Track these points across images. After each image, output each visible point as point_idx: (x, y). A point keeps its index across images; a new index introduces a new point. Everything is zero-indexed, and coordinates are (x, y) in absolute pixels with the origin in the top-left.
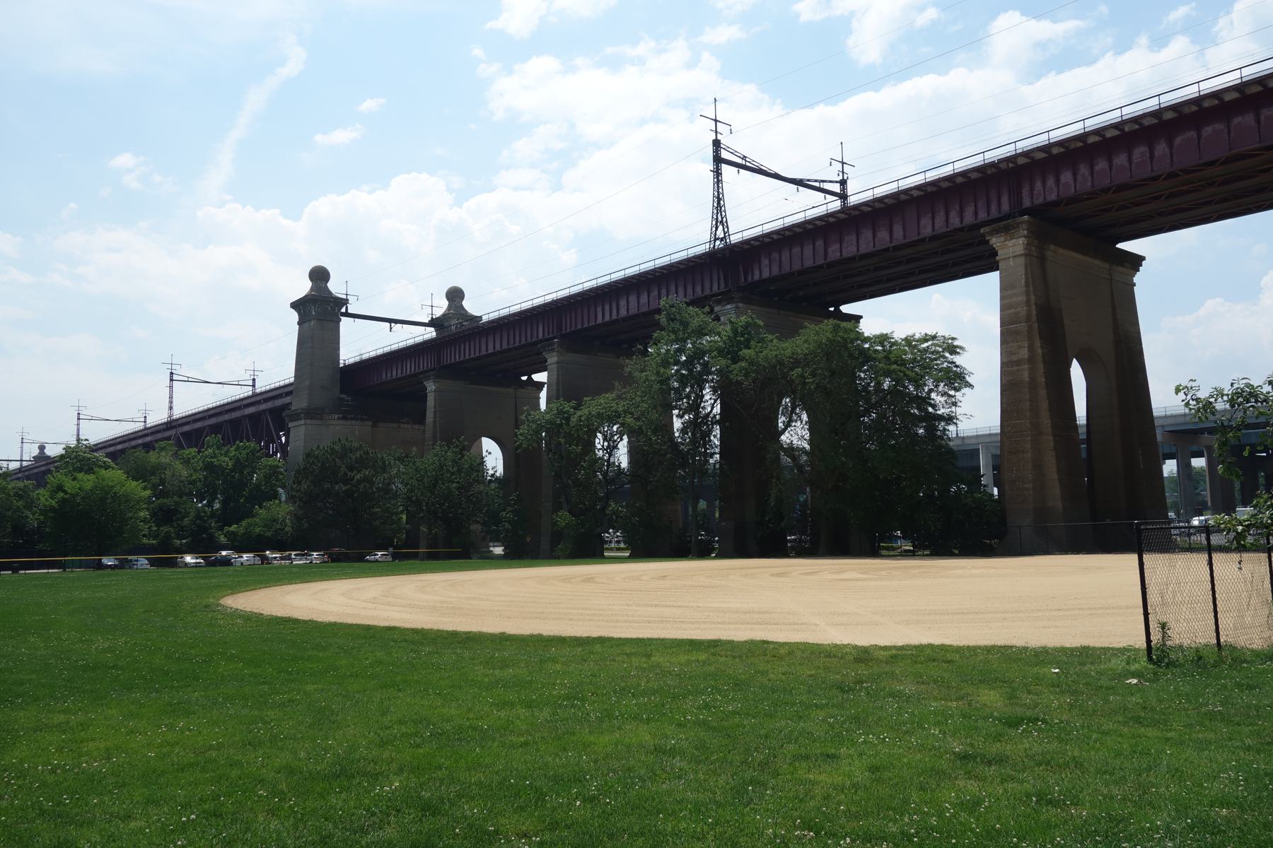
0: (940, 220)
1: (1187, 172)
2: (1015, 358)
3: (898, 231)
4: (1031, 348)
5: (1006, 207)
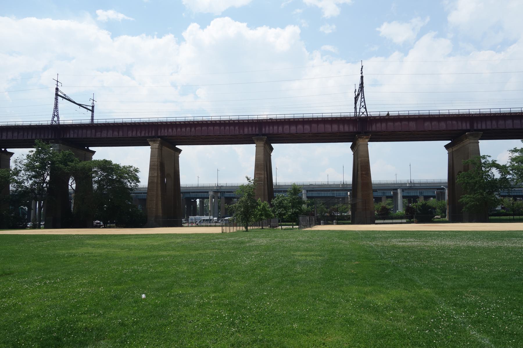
1: (197, 136)
2: (153, 175)
3: (121, 133)
4: (157, 173)
5: (153, 134)
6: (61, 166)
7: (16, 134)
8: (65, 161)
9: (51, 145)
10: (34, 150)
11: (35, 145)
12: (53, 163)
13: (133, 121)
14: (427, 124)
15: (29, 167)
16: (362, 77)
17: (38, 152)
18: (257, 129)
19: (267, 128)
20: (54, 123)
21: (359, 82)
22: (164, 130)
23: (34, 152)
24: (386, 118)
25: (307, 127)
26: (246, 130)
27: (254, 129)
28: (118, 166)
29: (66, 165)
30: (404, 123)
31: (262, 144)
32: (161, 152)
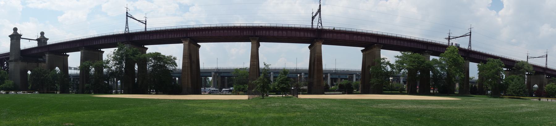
0: (173, 36)
4: (188, 61)
5: (185, 36)
6: (132, 57)
7: (106, 40)
8: (134, 54)
9: (125, 45)
10: (117, 49)
11: (118, 45)
12: (127, 56)
13: (172, 28)
14: (355, 37)
15: (115, 59)
16: (320, 5)
17: (119, 50)
18: (252, 32)
19: (259, 32)
20: (126, 32)
21: (318, 8)
22: (192, 33)
23: (117, 50)
24: (334, 31)
25: (285, 33)
26: (245, 33)
27: (250, 32)
28: (164, 56)
29: (134, 57)
30: (342, 35)
31: (255, 42)
32: (190, 47)
